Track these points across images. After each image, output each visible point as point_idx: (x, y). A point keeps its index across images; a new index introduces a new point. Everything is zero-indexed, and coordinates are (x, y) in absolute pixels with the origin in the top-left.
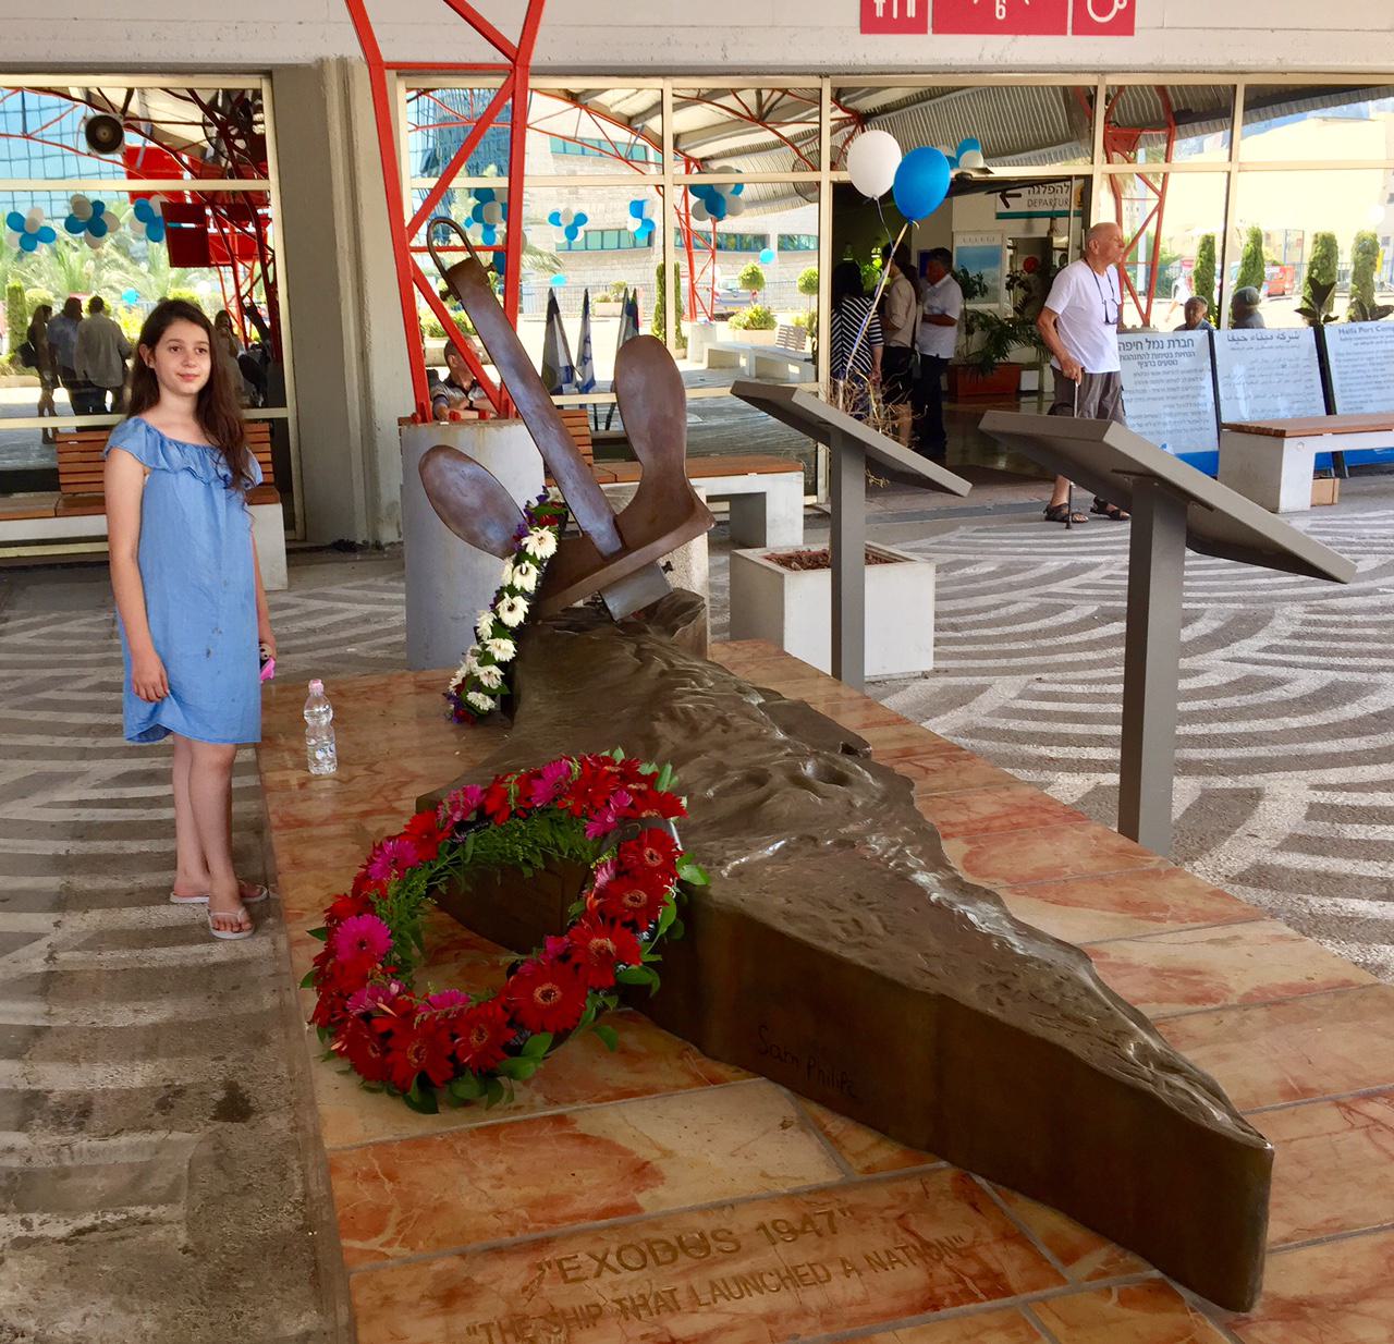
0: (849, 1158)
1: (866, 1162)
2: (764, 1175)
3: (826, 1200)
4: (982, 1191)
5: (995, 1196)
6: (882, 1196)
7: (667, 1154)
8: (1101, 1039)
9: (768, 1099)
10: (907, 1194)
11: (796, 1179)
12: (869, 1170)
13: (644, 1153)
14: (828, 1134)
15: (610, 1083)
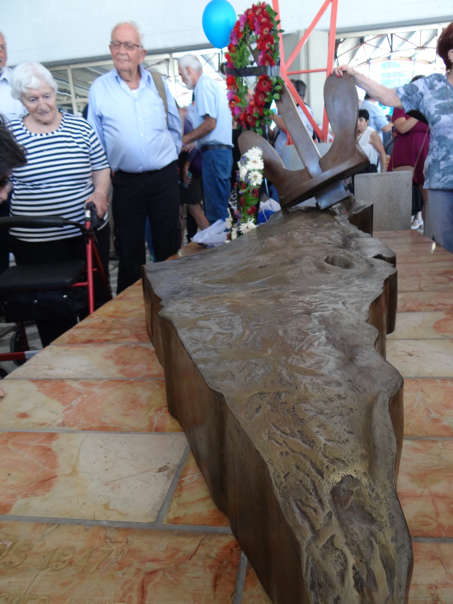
0: (174, 505)
1: (181, 513)
2: (106, 507)
3: (120, 539)
4: (237, 567)
5: (243, 574)
6: (160, 546)
7: (74, 472)
8: (314, 465)
9: (173, 446)
10: (178, 551)
11: (121, 514)
12: (176, 520)
13: (63, 468)
14: (180, 483)
15: (103, 420)
